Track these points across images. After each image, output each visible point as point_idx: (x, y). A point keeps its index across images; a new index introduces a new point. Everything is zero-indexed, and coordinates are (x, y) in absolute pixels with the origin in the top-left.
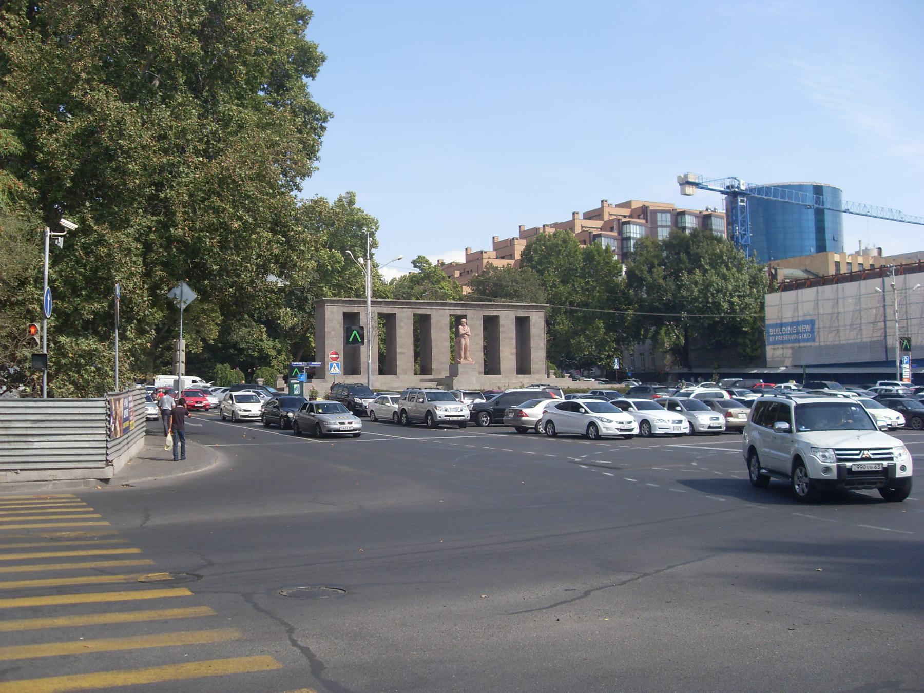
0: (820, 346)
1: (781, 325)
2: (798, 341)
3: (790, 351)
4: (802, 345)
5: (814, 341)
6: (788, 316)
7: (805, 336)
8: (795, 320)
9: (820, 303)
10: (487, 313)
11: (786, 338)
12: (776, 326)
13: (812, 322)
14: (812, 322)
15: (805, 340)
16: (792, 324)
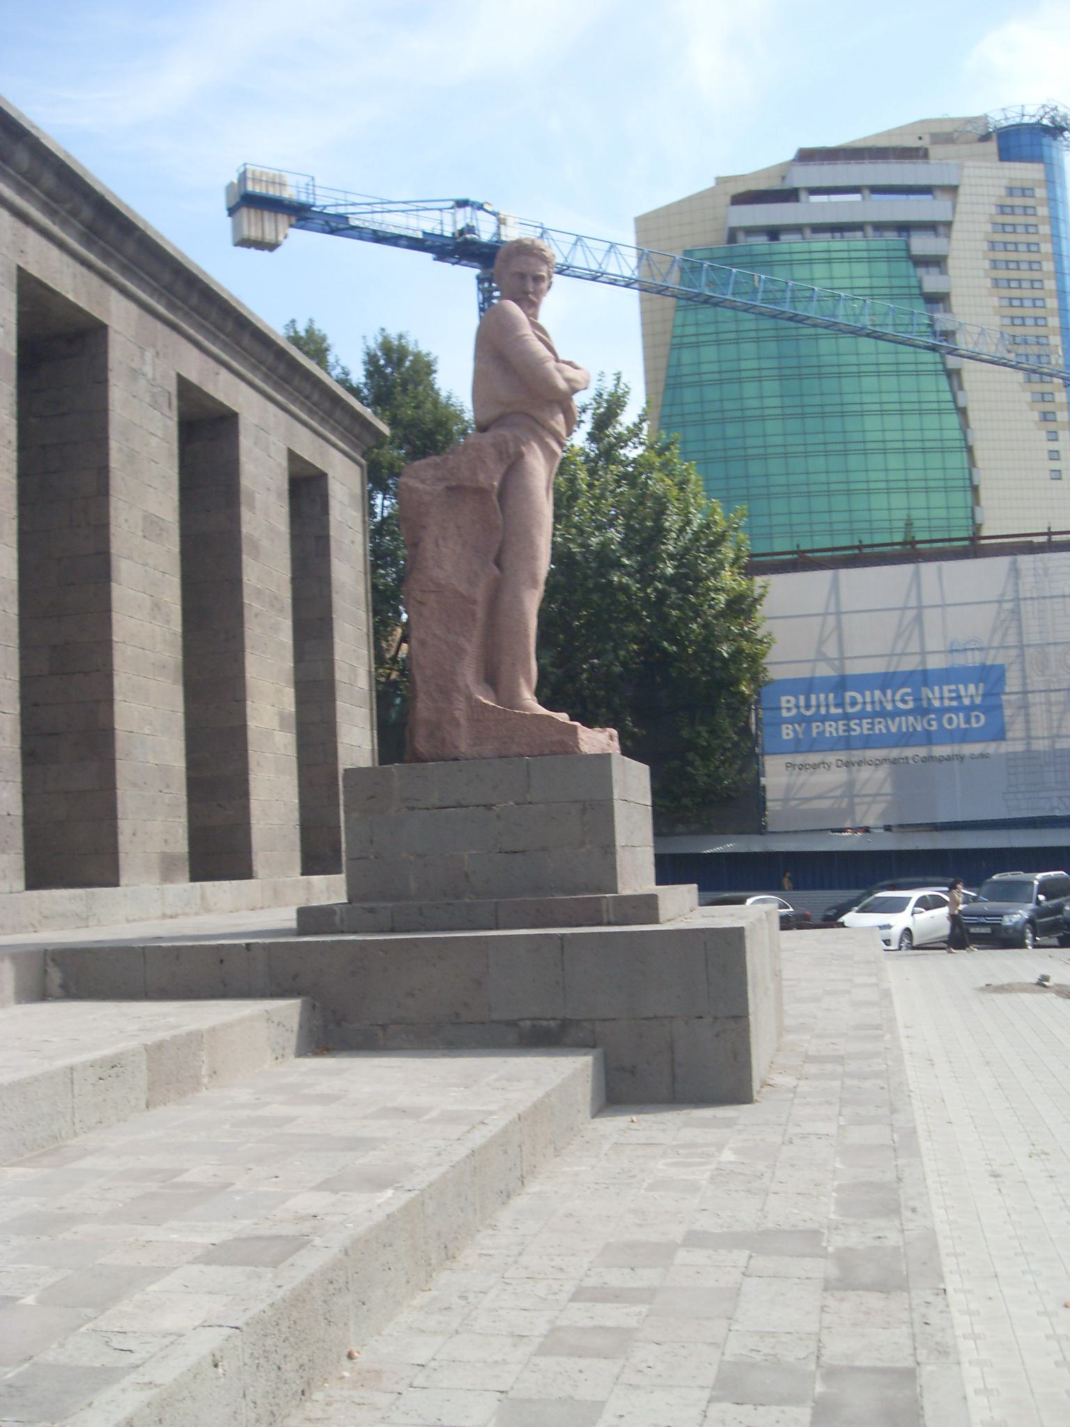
0: (1029, 755)
1: (841, 684)
2: (928, 739)
3: (882, 773)
4: (941, 751)
5: (1000, 736)
6: (869, 647)
7: (959, 721)
8: (909, 664)
9: (1027, 608)
10: (196, 367)
11: (860, 728)
12: (808, 686)
13: (991, 677)
14: (991, 677)
15: (964, 736)
16: (887, 681)
